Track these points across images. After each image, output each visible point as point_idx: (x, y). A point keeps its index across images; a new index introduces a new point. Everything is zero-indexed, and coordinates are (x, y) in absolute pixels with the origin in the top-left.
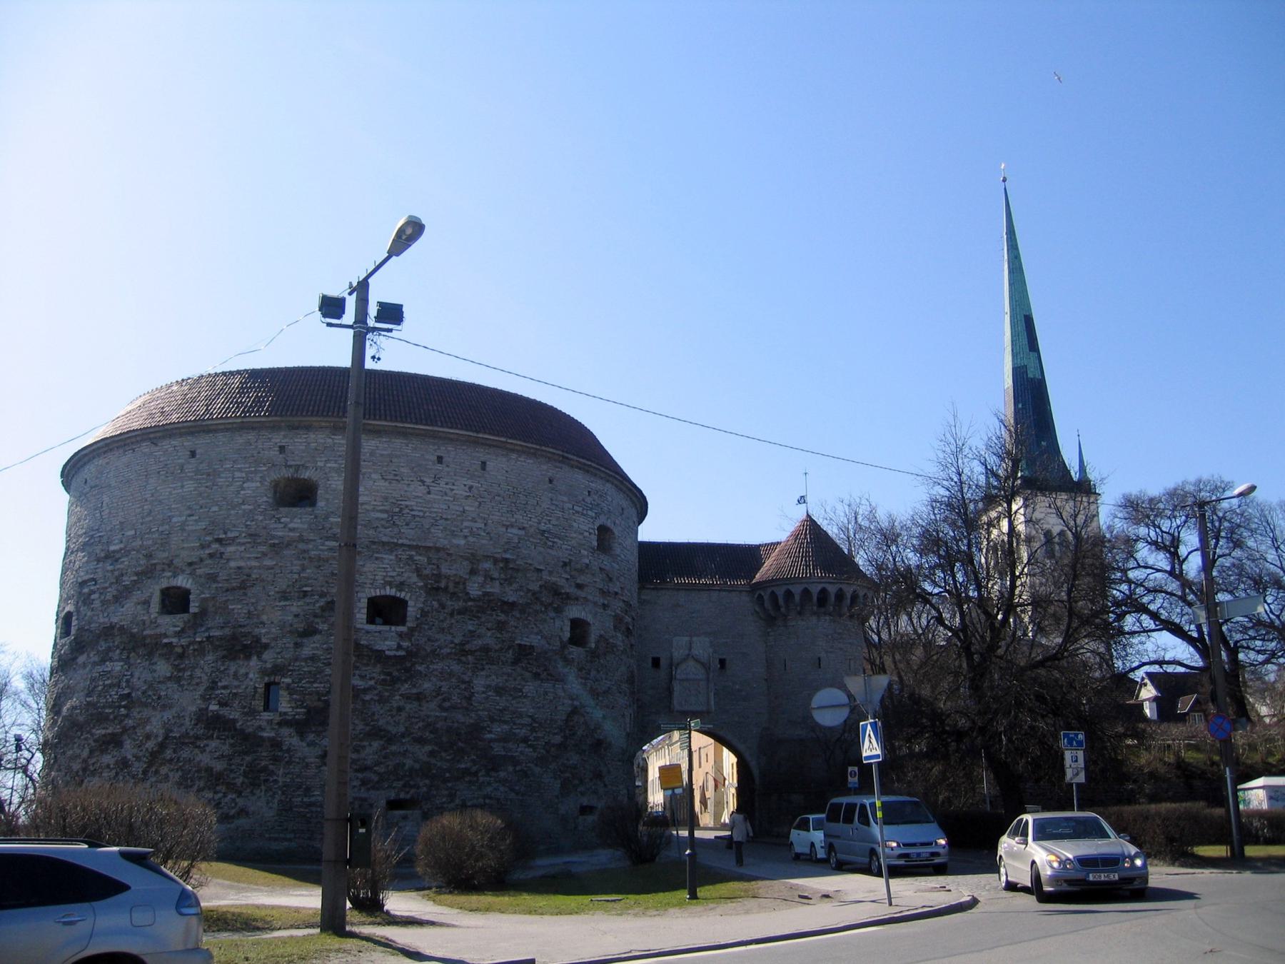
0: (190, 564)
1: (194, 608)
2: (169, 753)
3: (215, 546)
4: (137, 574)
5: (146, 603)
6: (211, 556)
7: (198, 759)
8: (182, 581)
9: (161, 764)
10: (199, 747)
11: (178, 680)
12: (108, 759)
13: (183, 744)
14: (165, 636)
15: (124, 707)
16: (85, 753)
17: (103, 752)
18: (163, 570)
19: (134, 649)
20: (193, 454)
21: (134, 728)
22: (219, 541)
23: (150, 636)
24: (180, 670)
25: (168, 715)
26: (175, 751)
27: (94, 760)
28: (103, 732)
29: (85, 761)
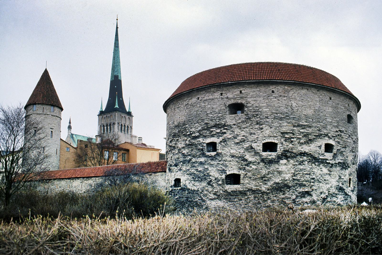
0: (333, 137)
1: (335, 151)
2: (329, 199)
3: (339, 133)
4: (315, 136)
5: (320, 147)
6: (338, 135)
7: (337, 201)
8: (331, 142)
9: (327, 203)
10: (336, 197)
11: (330, 174)
12: (304, 200)
13: (333, 196)
14: (327, 160)
15: (313, 182)
16: (294, 197)
17: (304, 197)
18: (324, 137)
19: (314, 163)
20: (330, 98)
21: (316, 190)
22: (340, 131)
23: (322, 159)
24: (330, 172)
25: (328, 186)
26: (331, 199)
27: (298, 200)
28: (303, 190)
29: (294, 200)
